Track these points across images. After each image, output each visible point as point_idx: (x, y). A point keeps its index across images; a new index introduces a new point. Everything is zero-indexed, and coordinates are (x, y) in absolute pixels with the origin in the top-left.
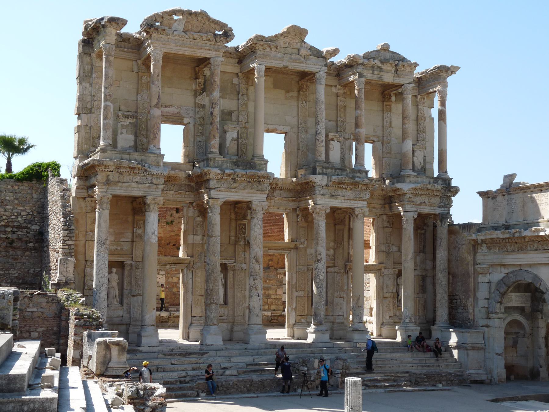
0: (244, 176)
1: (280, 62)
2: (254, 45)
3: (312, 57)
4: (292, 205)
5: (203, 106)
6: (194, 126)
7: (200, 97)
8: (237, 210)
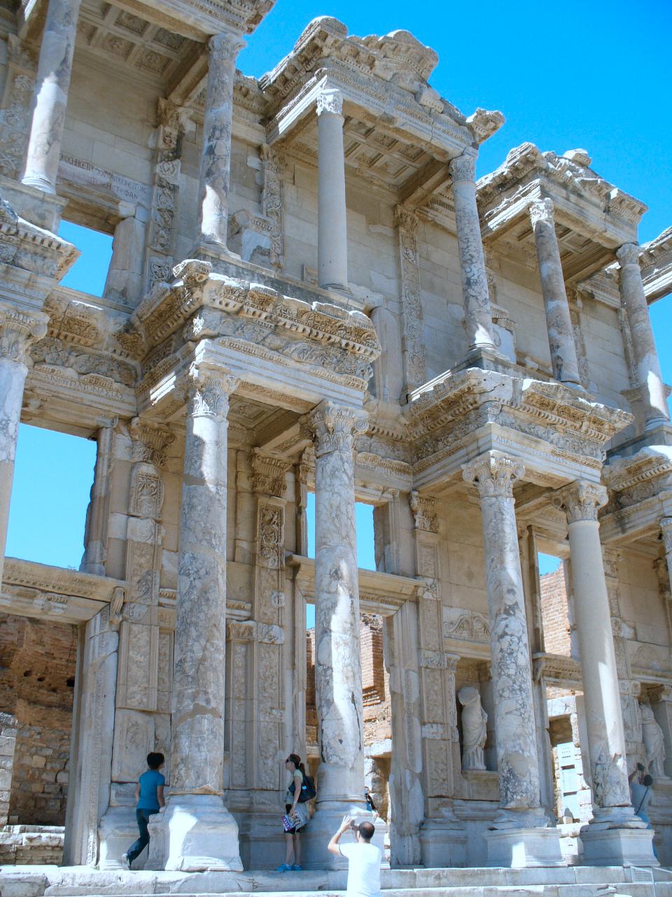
0: (304, 317)
1: (377, 101)
2: (318, 42)
3: (445, 117)
4: (401, 483)
5: (174, 189)
6: (146, 225)
7: (166, 166)
8: (257, 463)
